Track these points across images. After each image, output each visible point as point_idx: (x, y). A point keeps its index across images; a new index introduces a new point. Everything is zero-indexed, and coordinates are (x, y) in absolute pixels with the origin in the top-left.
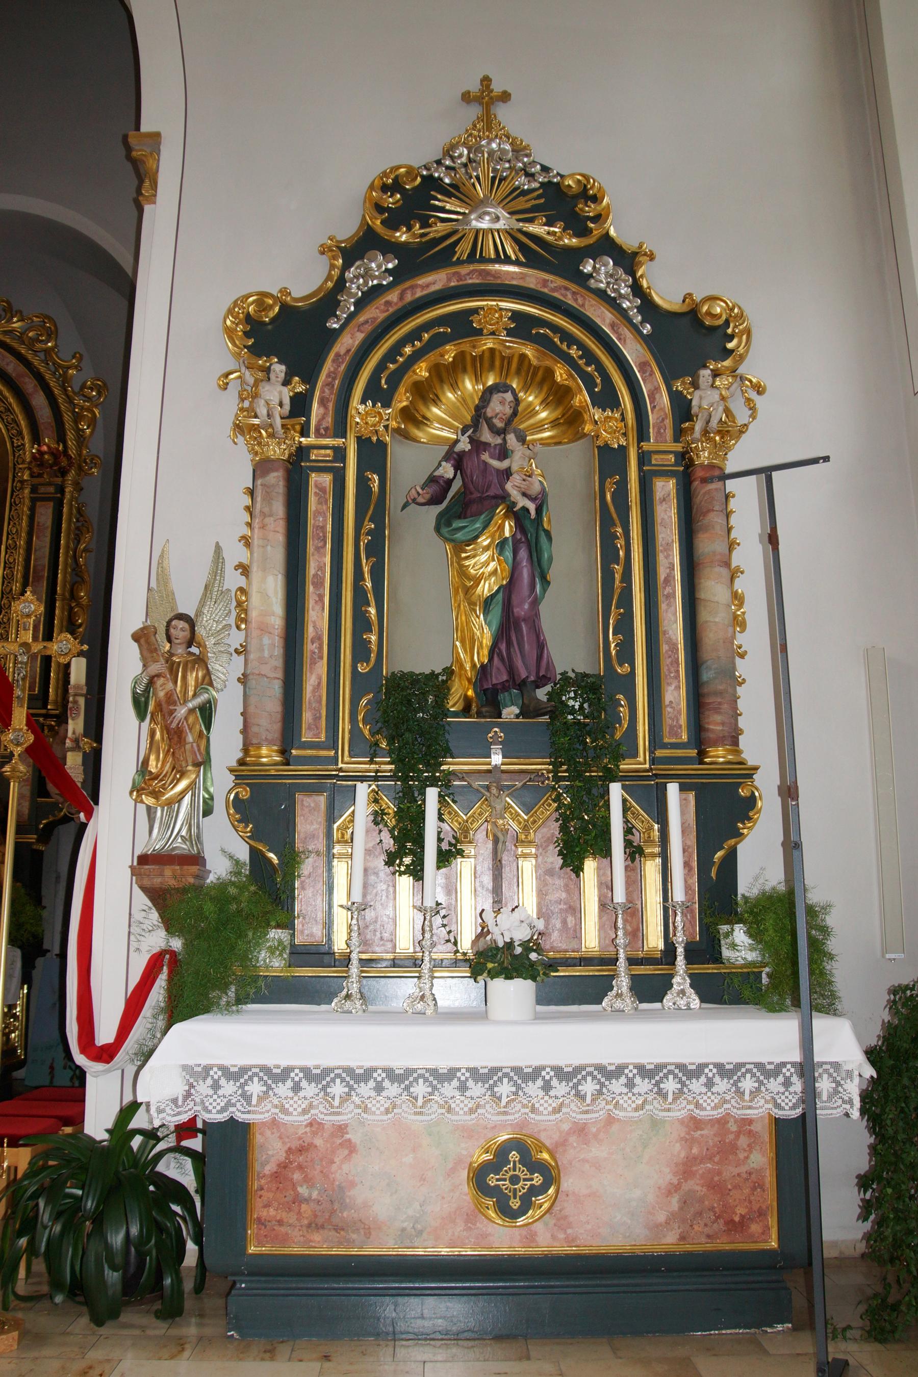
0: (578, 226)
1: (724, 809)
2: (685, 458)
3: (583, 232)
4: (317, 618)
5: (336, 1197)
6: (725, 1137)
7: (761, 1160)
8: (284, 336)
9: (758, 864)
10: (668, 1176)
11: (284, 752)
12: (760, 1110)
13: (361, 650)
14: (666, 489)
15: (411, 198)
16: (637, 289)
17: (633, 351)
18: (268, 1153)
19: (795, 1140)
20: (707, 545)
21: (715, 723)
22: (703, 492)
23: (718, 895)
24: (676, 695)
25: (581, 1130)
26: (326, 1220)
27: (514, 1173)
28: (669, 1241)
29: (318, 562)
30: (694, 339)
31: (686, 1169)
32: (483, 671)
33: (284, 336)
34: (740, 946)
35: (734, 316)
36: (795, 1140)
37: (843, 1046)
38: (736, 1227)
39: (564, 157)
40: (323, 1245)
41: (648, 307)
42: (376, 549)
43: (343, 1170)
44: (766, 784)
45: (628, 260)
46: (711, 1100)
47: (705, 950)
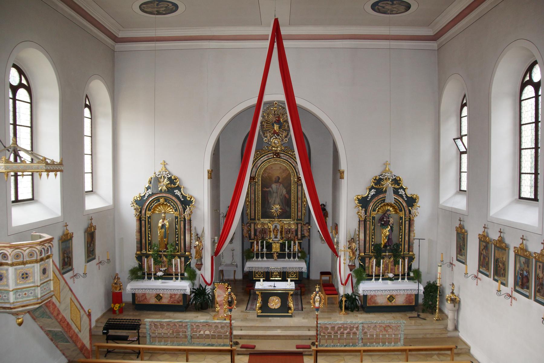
0: (398, 184)
1: (411, 259)
2: (410, 219)
3: (399, 185)
4: (368, 238)
5: (375, 300)
6: (410, 295)
7: (414, 297)
8: (364, 202)
9: (415, 266)
10: (404, 298)
11: (365, 252)
12: (414, 293)
13: (372, 241)
14: (407, 222)
15: (378, 181)
16: (405, 194)
17: (404, 204)
18: (369, 298)
19: (417, 296)
20: (411, 229)
21: (411, 250)
22: (412, 222)
23: (410, 268)
24: (406, 246)
25: (397, 295)
26: (374, 303)
27: (391, 298)
28: (405, 304)
29: (368, 232)
30: (412, 201)
31: (406, 298)
32: (385, 244)
33: (364, 202)
34: (412, 274)
35: (417, 197)
36: (417, 296)
37: (422, 288)
38: (411, 303)
39: (397, 172)
40: (374, 305)
41: (407, 196)
42: (374, 229)
43: (376, 298)
44: (416, 257)
45: (404, 190)
46: (409, 292)
47: (408, 275)
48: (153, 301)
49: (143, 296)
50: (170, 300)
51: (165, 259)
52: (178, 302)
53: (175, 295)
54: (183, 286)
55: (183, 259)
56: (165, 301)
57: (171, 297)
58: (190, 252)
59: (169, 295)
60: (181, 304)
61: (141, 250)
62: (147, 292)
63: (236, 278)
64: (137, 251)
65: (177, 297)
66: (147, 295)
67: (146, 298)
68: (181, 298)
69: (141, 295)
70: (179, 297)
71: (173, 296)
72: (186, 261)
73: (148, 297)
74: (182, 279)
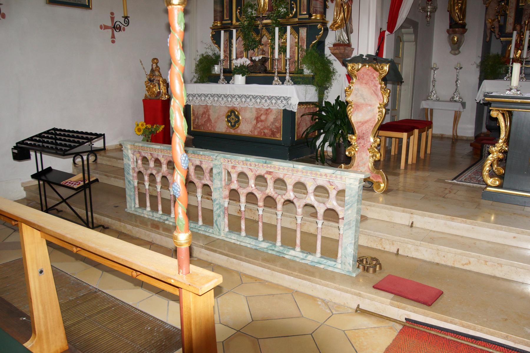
48: (221, 127)
49: (204, 113)
50: (255, 127)
51: (264, 32)
52: (273, 133)
53: (268, 111)
54: (292, 95)
55: (303, 32)
56: (245, 129)
57: (258, 119)
58: (324, 13)
59: (254, 115)
60: (279, 137)
61: (222, 19)
62: (209, 102)
63: (460, 133)
64: (215, 20)
65: (271, 118)
66: (211, 112)
67: (209, 120)
68: (280, 124)
69: (201, 111)
70: (276, 120)
71: (263, 117)
72: (310, 37)
73: (213, 117)
74: (296, 81)
